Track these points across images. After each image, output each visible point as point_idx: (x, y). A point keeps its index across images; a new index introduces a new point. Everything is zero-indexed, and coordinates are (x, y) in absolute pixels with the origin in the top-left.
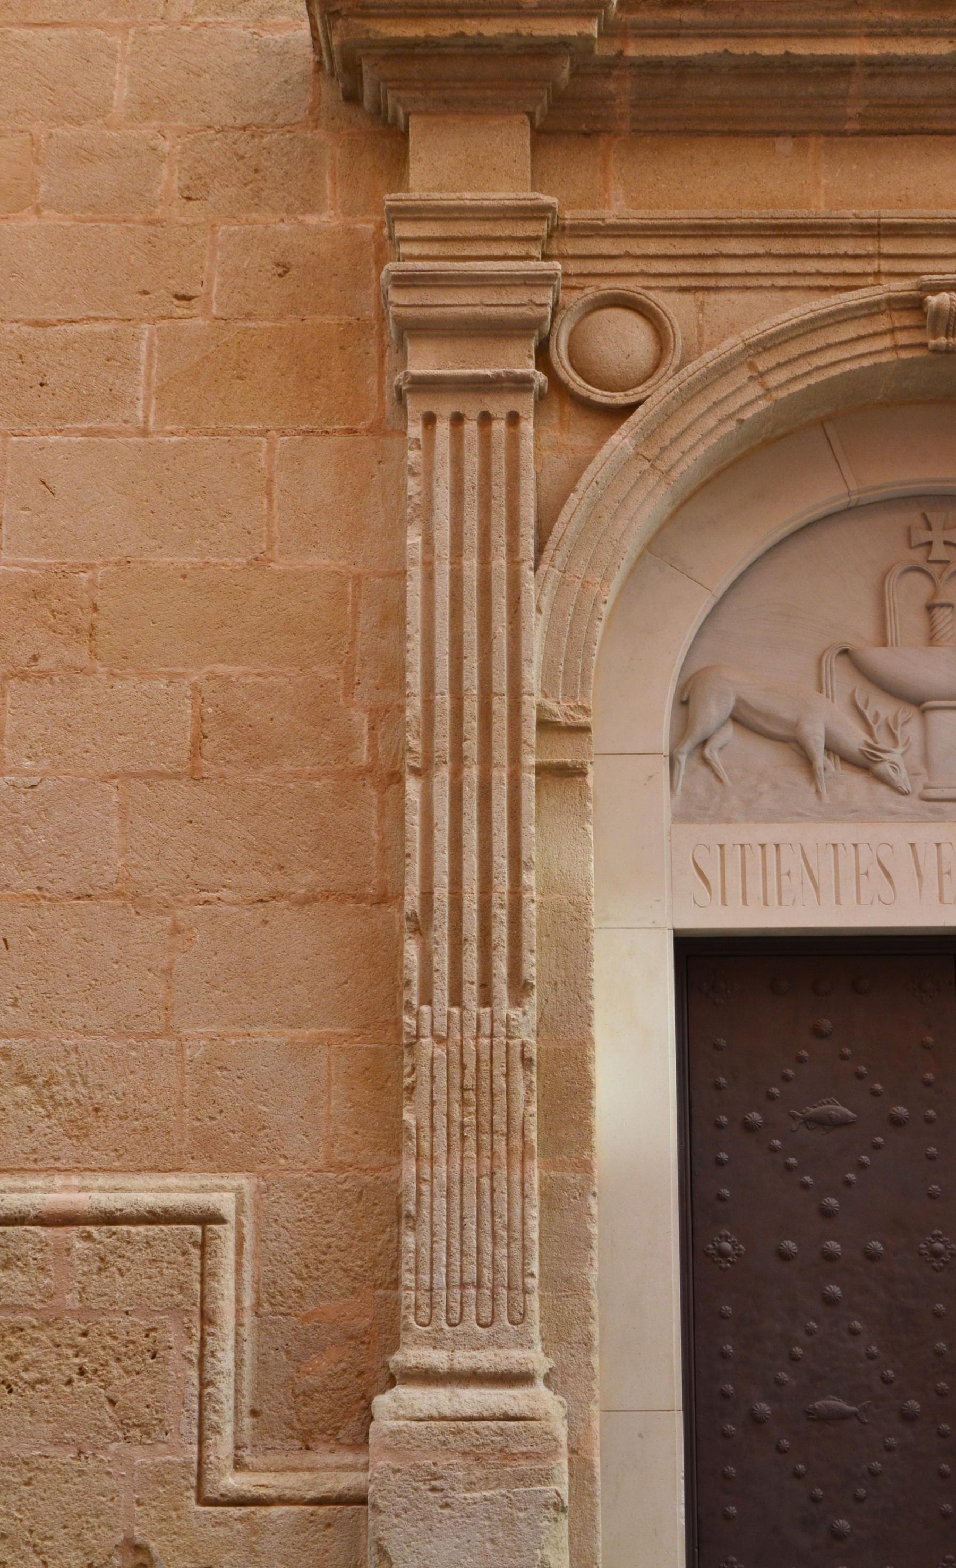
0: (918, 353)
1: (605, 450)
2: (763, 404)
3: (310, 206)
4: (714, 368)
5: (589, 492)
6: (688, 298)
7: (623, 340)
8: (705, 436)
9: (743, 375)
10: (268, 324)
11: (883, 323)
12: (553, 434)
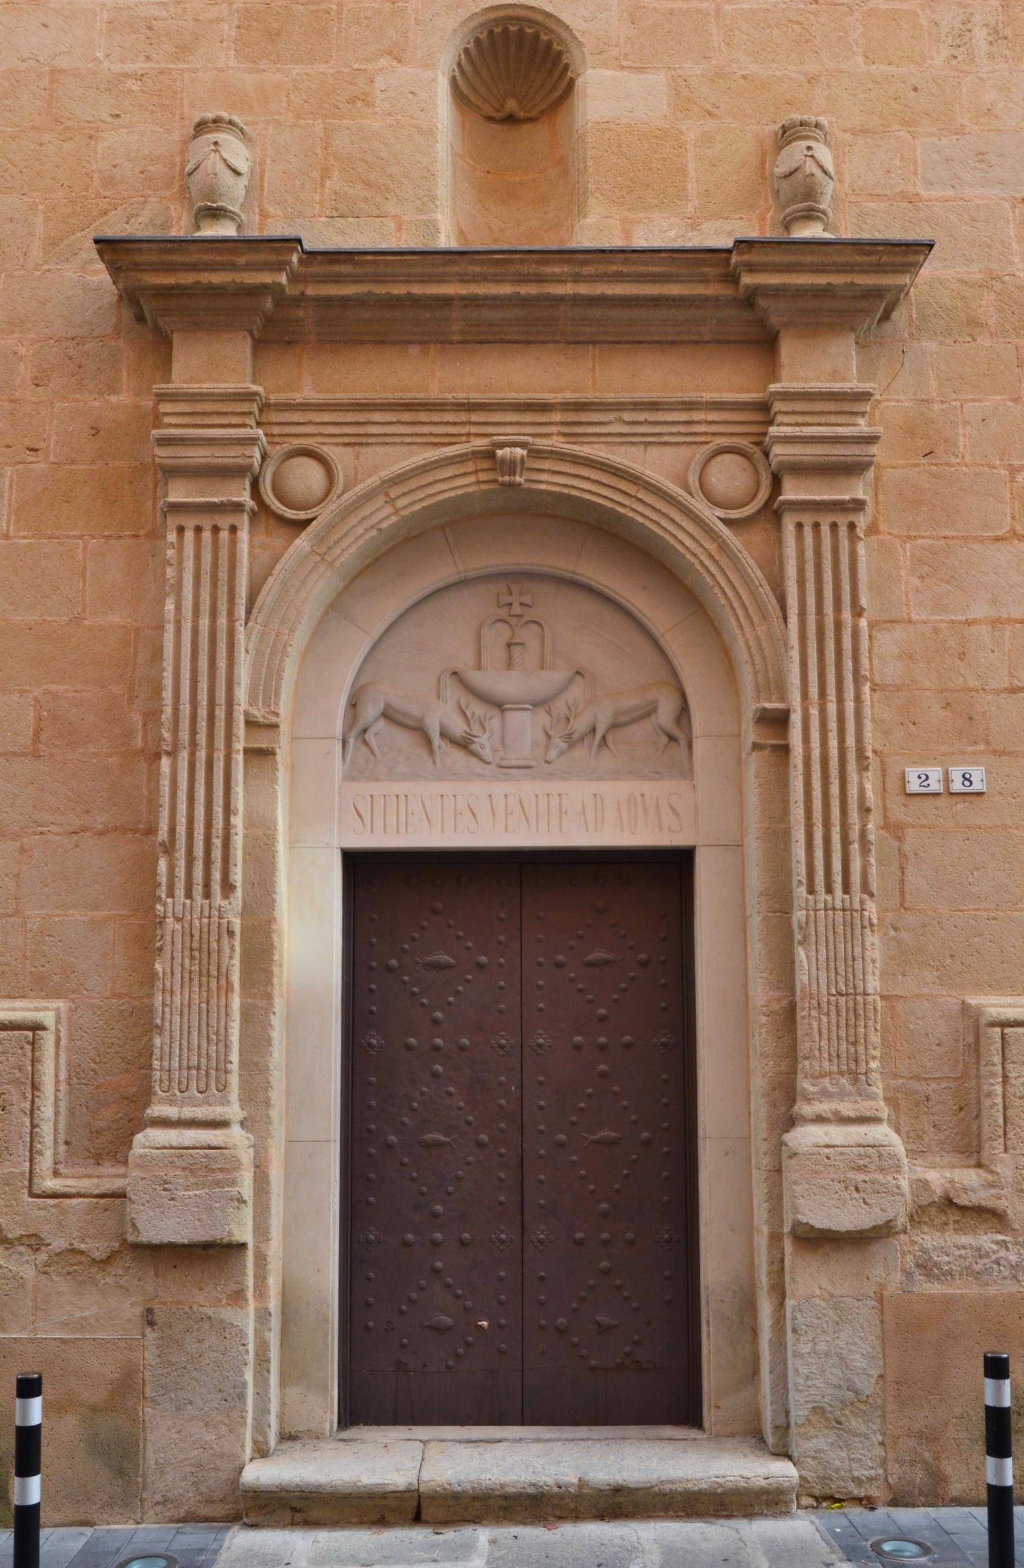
0: (492, 486)
1: (291, 549)
2: (394, 519)
3: (113, 390)
4: (362, 496)
5: (281, 577)
6: (350, 450)
7: (306, 477)
8: (357, 539)
9: (380, 501)
10: (85, 467)
11: (470, 467)
12: (261, 538)
